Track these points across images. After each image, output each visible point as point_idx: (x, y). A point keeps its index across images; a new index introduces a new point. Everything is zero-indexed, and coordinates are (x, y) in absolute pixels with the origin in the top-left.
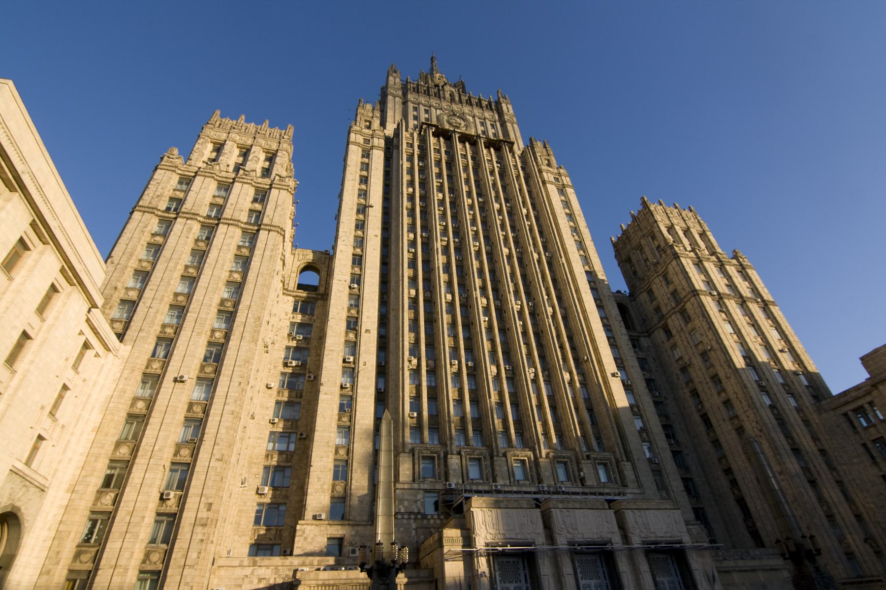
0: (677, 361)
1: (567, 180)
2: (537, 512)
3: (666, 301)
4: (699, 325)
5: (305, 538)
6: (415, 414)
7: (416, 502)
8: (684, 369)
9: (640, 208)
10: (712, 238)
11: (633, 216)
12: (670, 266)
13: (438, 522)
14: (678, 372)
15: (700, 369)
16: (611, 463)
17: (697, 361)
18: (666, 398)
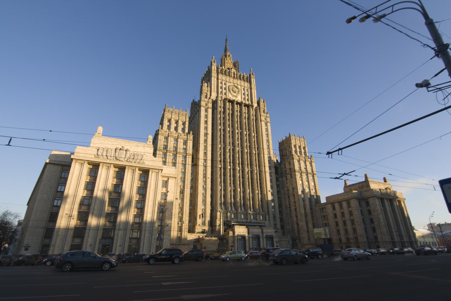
1: (268, 119)
10: (307, 149)
11: (286, 137)
17: (291, 189)
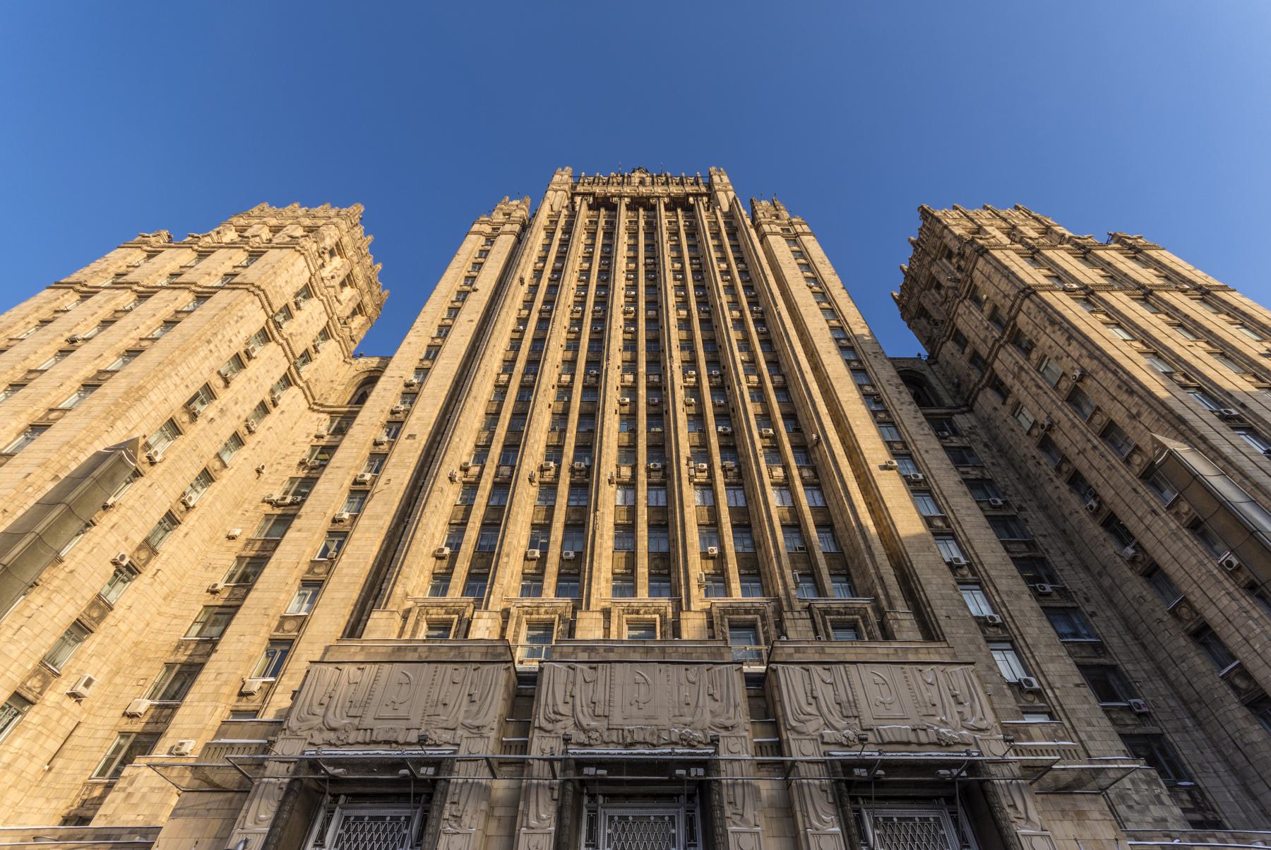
0: (1029, 433)
3: (982, 334)
5: (130, 795)
6: (447, 551)
8: (1046, 444)
12: (976, 273)
14: (1036, 452)
15: (1074, 426)
16: (865, 618)
17: (1064, 415)
18: (1021, 509)
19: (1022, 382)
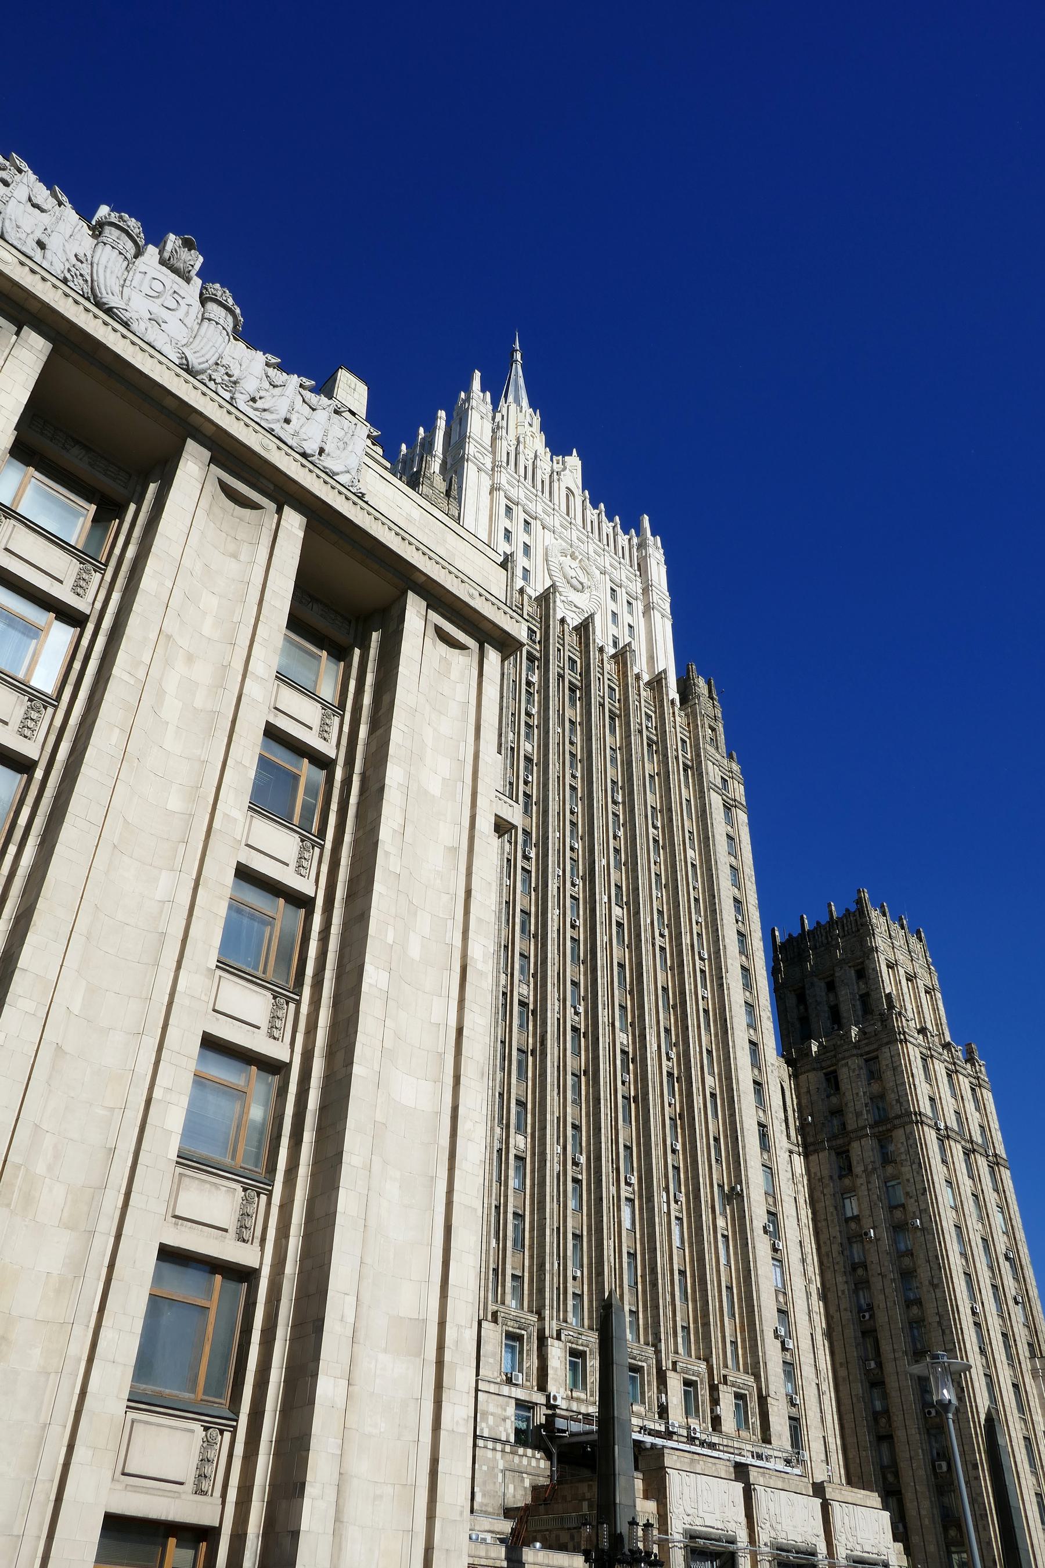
2: (740, 1486)
4: (909, 1176)
7: (504, 1420)
9: (853, 908)
13: (534, 1463)
19: (868, 1182)
